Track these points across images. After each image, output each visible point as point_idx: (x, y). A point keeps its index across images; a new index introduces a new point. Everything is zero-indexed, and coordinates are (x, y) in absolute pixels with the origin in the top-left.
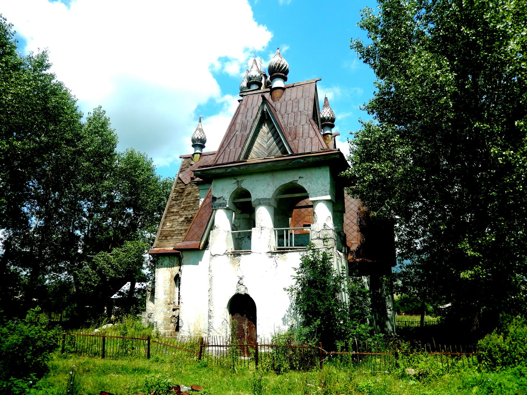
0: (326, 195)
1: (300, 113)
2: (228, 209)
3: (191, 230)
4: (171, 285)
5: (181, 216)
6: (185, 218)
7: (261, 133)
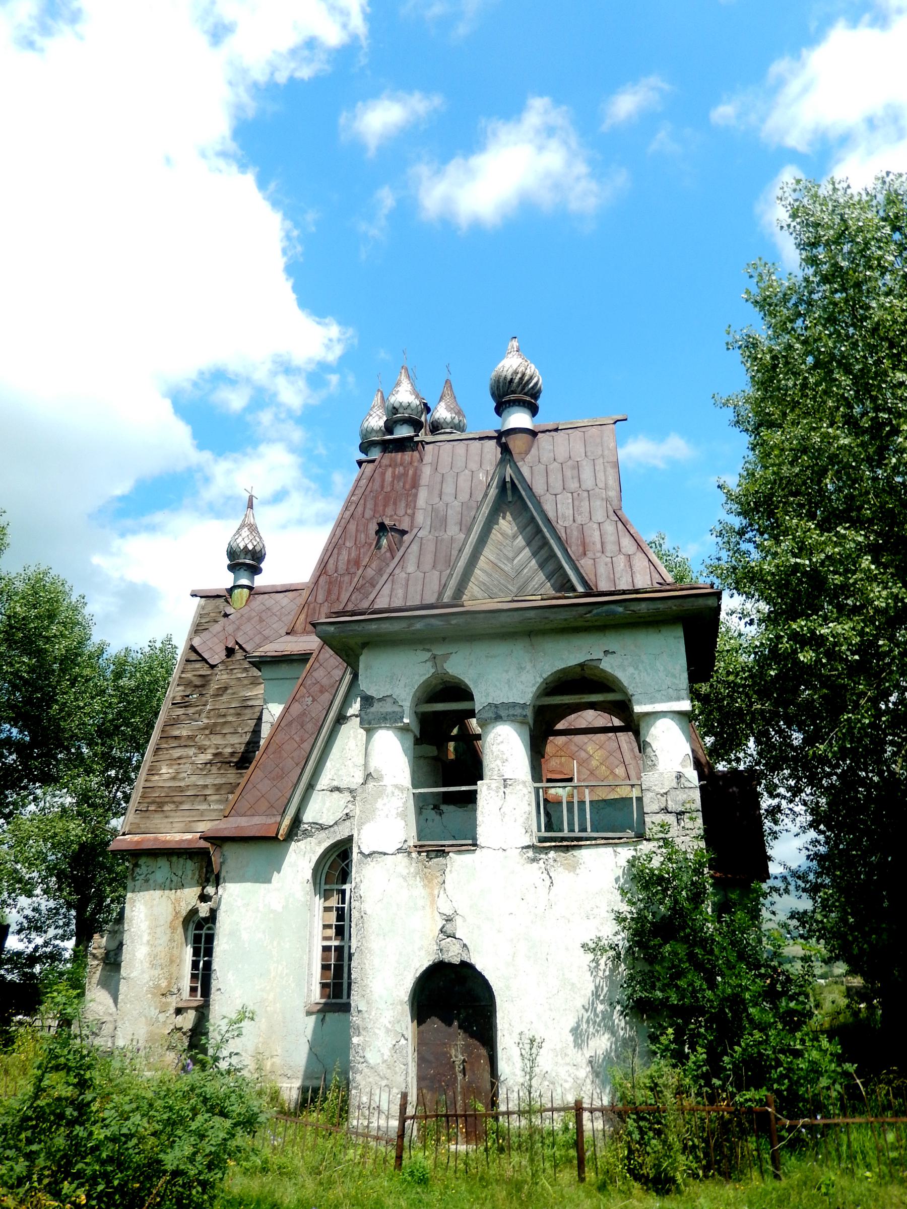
0: (678, 699)
1: (586, 494)
2: (405, 729)
3: (250, 786)
4: (172, 940)
5: (202, 749)
6: (215, 755)
7: (495, 535)
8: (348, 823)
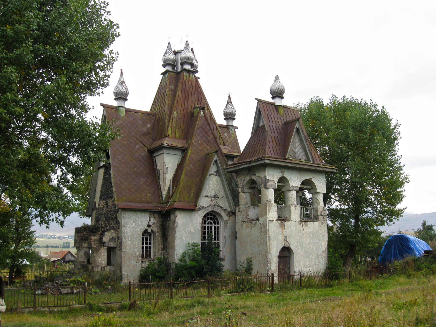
8: (210, 207)
